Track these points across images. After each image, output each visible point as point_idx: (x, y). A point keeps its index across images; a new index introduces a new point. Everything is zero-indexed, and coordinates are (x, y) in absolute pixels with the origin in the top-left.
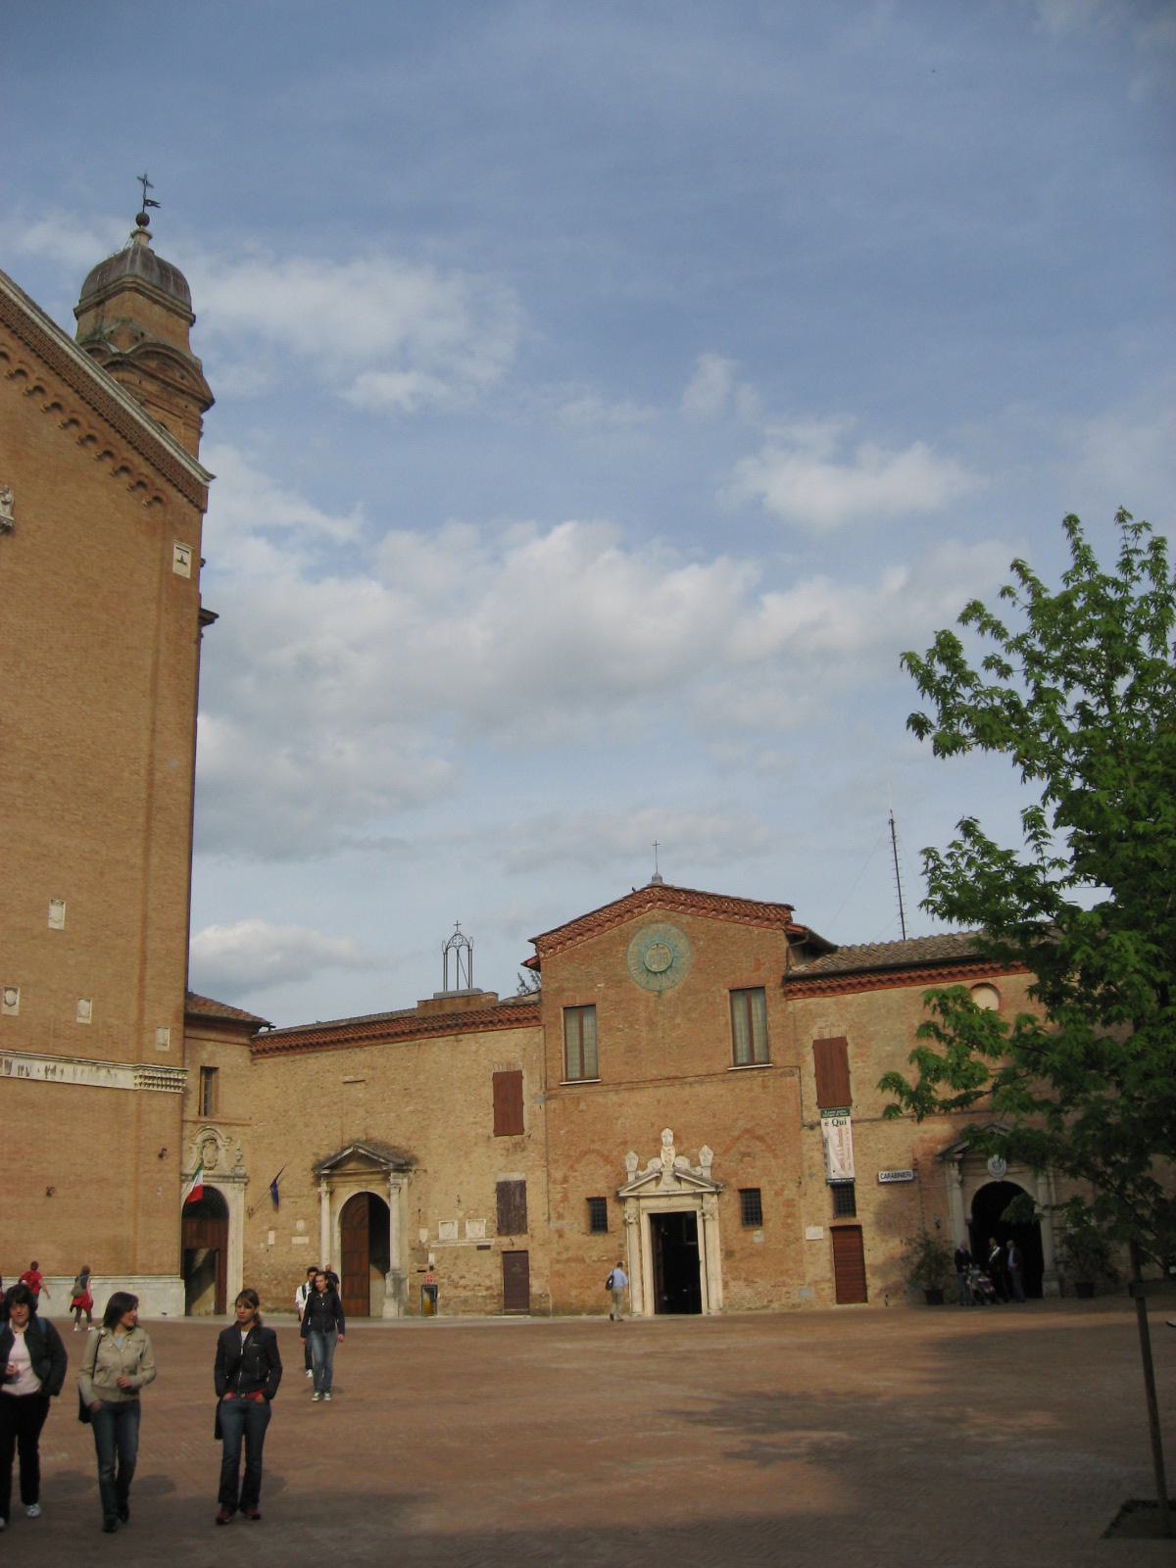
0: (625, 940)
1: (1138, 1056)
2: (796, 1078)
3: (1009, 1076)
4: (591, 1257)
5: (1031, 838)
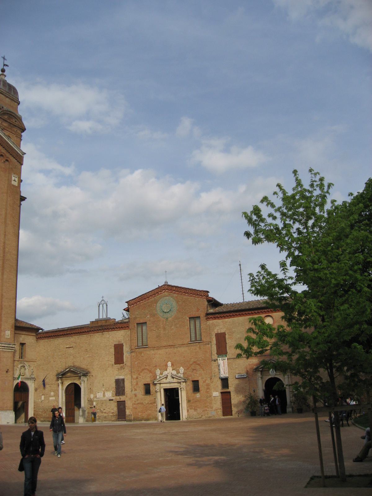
0: (156, 302)
1: (315, 338)
2: (210, 345)
3: (275, 344)
4: (145, 403)
5: (282, 270)
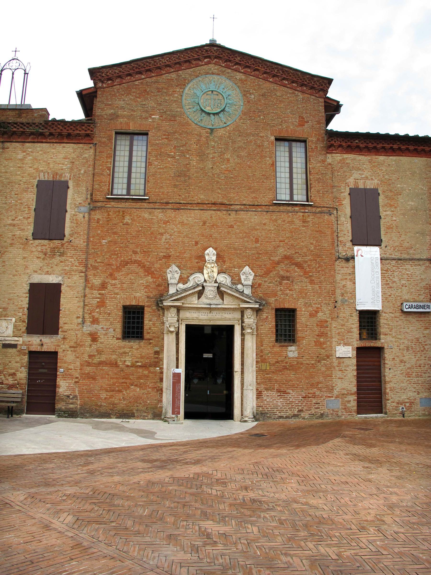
0: (183, 84)
4: (125, 361)
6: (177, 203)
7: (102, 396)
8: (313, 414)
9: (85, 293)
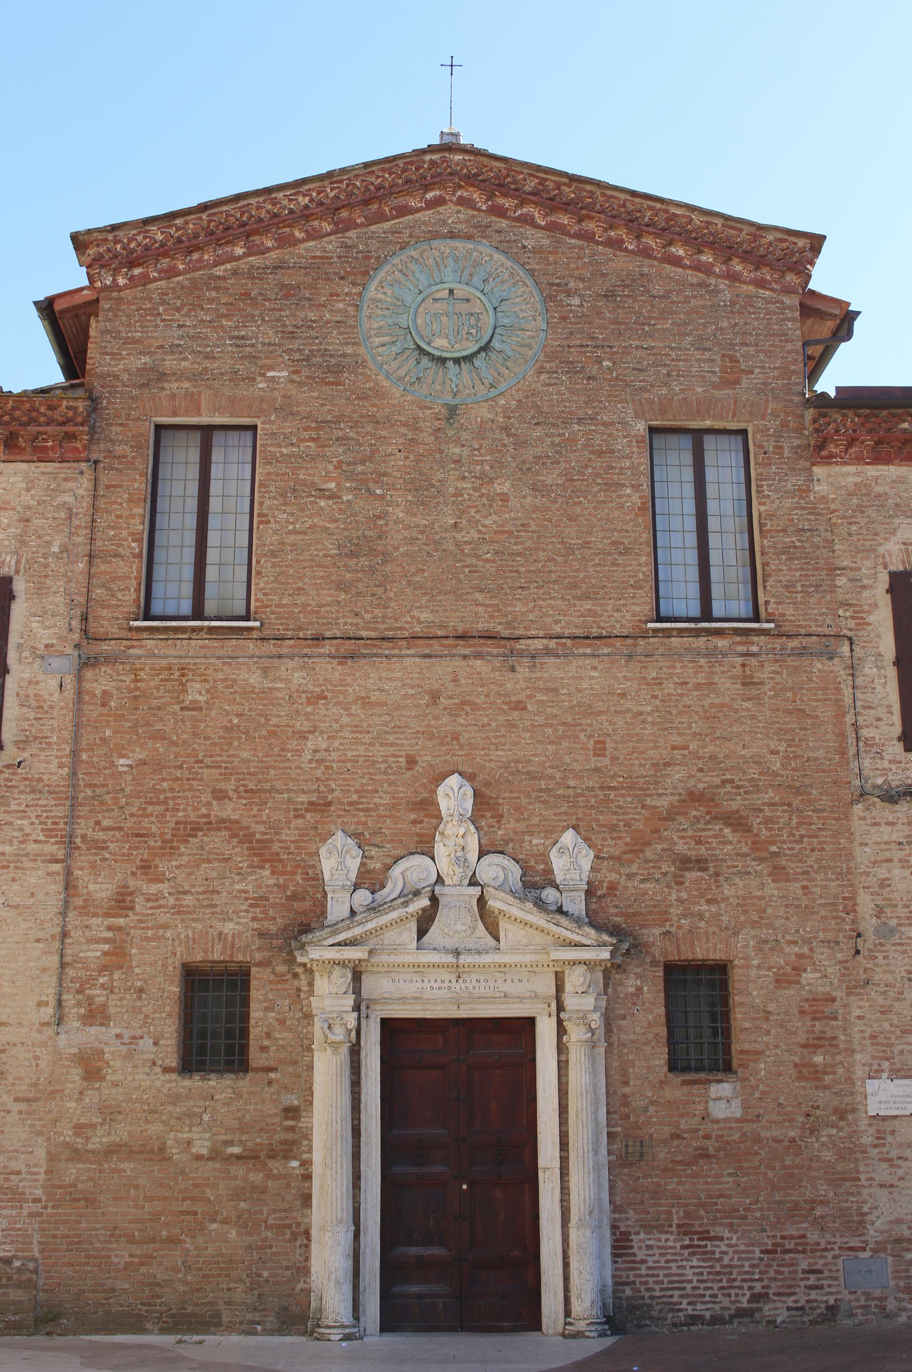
6: (350, 639)
7: (116, 1260)
8: (802, 1308)
9: (64, 926)
